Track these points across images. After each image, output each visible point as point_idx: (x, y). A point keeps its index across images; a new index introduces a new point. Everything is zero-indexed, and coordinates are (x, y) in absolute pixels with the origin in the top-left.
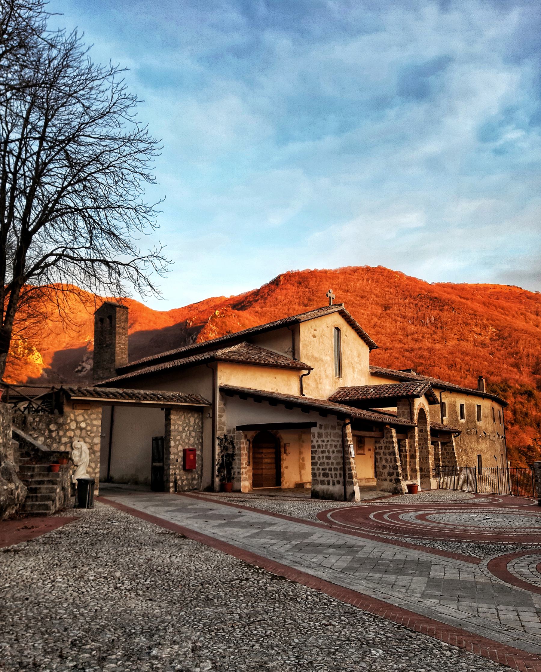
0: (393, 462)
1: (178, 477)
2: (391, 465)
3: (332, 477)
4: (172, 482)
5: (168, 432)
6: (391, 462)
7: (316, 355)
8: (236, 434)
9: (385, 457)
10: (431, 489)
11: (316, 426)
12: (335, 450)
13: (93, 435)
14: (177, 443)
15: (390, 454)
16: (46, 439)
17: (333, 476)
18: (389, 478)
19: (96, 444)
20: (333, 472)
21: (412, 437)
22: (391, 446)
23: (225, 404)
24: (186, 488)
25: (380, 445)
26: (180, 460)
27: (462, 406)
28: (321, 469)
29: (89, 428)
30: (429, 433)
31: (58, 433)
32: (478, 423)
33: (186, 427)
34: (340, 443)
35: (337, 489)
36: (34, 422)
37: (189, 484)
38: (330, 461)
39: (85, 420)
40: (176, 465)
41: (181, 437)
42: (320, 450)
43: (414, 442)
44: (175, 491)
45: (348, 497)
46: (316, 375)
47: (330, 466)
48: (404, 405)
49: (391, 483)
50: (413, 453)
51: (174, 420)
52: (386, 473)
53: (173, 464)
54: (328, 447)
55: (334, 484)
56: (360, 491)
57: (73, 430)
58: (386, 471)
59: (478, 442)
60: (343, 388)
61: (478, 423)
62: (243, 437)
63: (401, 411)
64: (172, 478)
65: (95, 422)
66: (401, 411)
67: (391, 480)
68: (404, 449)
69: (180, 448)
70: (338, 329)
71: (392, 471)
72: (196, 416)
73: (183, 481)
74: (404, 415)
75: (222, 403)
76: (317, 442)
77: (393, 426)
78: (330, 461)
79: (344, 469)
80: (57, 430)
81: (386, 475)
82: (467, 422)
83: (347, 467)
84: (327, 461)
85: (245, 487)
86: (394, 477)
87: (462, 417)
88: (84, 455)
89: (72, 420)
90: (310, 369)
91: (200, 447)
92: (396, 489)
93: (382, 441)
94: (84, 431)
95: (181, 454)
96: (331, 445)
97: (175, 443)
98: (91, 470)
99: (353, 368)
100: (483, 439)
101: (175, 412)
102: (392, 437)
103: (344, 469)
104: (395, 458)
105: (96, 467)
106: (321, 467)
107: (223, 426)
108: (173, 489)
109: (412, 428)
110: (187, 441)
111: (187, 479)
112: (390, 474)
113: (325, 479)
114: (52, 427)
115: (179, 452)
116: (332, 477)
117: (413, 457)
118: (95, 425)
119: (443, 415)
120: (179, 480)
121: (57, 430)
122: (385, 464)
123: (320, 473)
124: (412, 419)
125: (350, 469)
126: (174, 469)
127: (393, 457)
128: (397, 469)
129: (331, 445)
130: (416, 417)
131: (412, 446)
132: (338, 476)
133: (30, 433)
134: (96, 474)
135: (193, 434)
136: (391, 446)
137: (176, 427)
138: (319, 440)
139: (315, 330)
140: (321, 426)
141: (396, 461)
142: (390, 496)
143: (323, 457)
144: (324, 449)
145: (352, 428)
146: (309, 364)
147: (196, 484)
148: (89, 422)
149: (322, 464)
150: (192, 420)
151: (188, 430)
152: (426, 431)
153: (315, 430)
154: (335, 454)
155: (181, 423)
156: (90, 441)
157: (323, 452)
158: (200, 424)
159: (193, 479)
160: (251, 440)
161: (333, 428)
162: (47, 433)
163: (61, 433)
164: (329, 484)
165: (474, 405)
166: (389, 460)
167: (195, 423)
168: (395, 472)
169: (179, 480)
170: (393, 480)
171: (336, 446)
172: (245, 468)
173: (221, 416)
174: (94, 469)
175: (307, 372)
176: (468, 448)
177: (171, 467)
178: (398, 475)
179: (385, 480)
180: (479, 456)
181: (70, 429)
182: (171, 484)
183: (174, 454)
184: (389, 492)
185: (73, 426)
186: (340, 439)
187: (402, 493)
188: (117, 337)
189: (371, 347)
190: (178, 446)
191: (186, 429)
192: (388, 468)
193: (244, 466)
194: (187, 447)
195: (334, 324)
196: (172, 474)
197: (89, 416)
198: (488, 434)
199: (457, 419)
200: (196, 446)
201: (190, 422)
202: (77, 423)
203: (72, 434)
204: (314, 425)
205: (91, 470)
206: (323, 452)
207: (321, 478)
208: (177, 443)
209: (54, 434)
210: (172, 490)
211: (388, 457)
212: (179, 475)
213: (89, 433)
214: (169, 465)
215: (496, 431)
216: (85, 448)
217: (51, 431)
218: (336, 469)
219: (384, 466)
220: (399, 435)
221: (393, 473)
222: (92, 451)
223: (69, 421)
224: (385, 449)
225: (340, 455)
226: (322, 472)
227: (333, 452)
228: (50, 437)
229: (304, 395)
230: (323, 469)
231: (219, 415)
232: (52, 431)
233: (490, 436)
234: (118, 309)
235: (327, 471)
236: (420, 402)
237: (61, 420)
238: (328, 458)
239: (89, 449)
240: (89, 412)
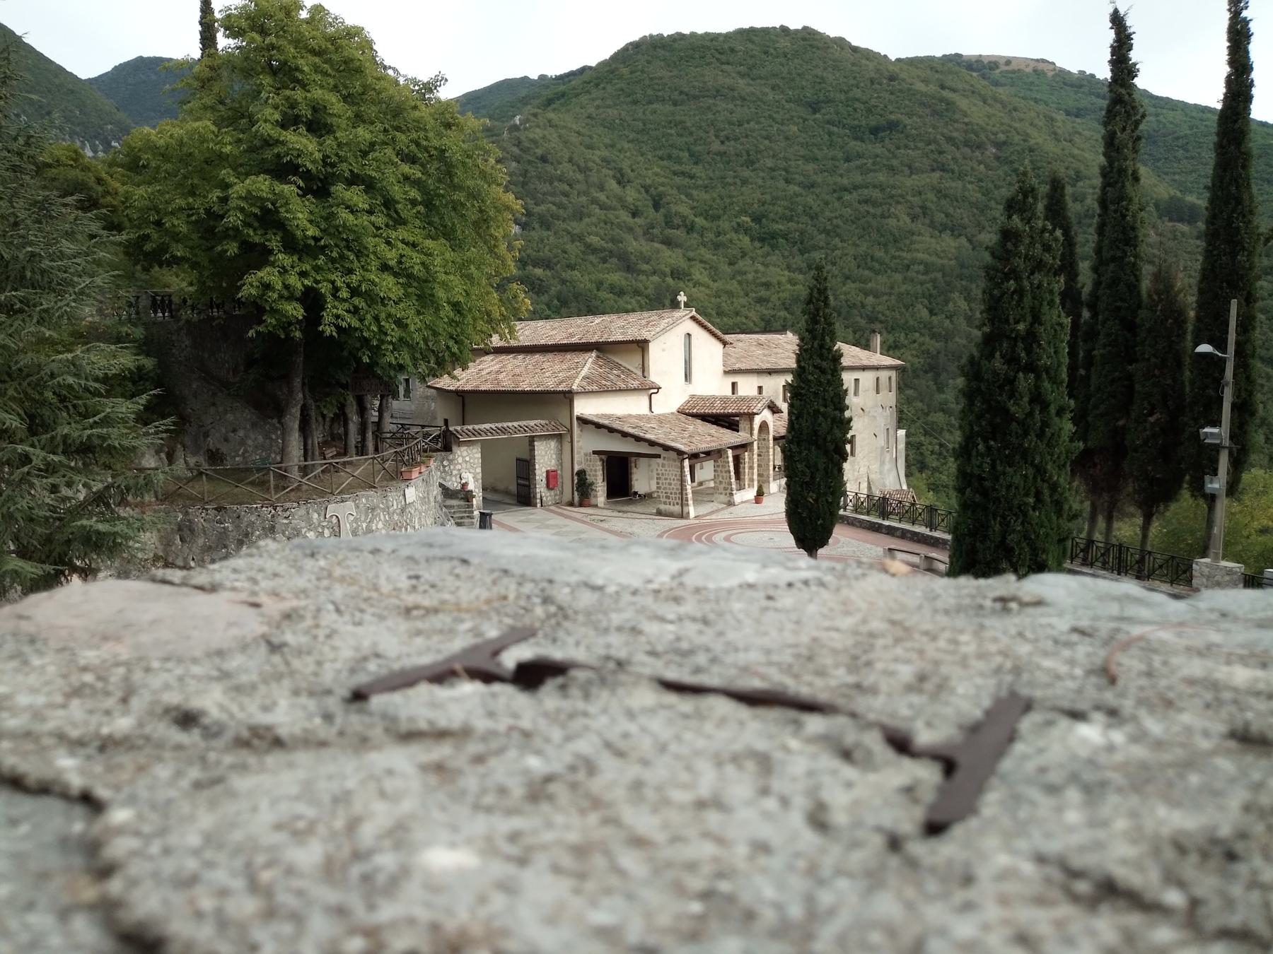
21: (752, 451)
35: (677, 509)
58: (722, 486)
60: (693, 396)
64: (538, 496)
86: (729, 491)
90: (659, 388)
114: (445, 463)
117: (751, 468)
124: (752, 434)
130: (756, 432)
131: (751, 459)
157: (666, 479)
161: (675, 461)
181: (458, 463)
185: (460, 460)
189: (725, 343)
198: (866, 410)
204: (658, 456)
206: (666, 479)
207: (664, 500)
209: (447, 469)
210: (539, 505)
217: (444, 466)
228: (444, 471)
237: (451, 457)
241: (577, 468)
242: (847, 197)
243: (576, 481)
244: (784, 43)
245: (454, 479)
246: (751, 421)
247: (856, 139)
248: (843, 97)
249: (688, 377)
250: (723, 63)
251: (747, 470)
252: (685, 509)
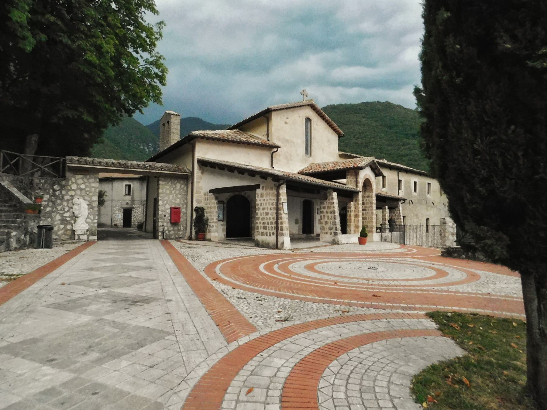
0: (333, 219)
1: (166, 228)
2: (332, 221)
3: (269, 230)
4: (160, 232)
5: (158, 194)
6: (331, 219)
7: (288, 138)
8: (209, 196)
9: (327, 215)
10: (373, 242)
11: (260, 188)
12: (272, 207)
13: (91, 194)
14: (165, 202)
15: (331, 213)
16: (51, 196)
17: (270, 228)
18: (329, 231)
19: (94, 202)
20: (270, 226)
21: (357, 201)
22: (332, 206)
23: (202, 173)
24: (173, 237)
25: (324, 205)
26: (167, 215)
27: (415, 183)
28: (262, 223)
29: (88, 189)
30: (374, 199)
31: (61, 192)
32: (428, 196)
33: (172, 191)
34: (275, 201)
35: (272, 239)
36: (40, 184)
37: (175, 234)
38: (268, 217)
39: (84, 183)
40: (164, 219)
41: (169, 198)
42: (261, 207)
43: (358, 204)
44: (163, 238)
45: (279, 246)
46: (287, 153)
47: (268, 221)
48: (351, 175)
49: (331, 236)
50: (357, 213)
51: (162, 185)
52: (328, 228)
53: (161, 218)
54: (268, 204)
55: (270, 235)
56: (291, 241)
57: (74, 190)
58: (327, 227)
59: (427, 209)
61: (428, 196)
62: (214, 198)
63: (349, 180)
65: (93, 185)
66: (349, 180)
67: (331, 234)
68: (349, 210)
69: (168, 206)
70: (308, 120)
71: (332, 226)
72: (182, 182)
73: (170, 231)
74: (351, 184)
75: (200, 172)
76: (260, 200)
77: (335, 190)
78: (268, 217)
79: (277, 223)
80: (61, 190)
81: (328, 229)
82: (419, 195)
83: (280, 221)
84: (266, 216)
85: (215, 237)
87: (415, 191)
88: (82, 209)
89: (73, 183)
90: (278, 147)
91: (185, 206)
92: (334, 240)
93: (325, 203)
94: (83, 191)
95: (169, 211)
96: (269, 203)
97: (163, 202)
98: (90, 221)
99: (323, 150)
100: (431, 207)
101: (163, 179)
102: (332, 199)
103: (277, 223)
104: (335, 216)
105: (94, 219)
107: (200, 190)
108: (162, 237)
109: (357, 193)
110: (174, 201)
111: (173, 230)
112: (330, 229)
113: (265, 231)
114: (56, 187)
115: (167, 209)
116: (269, 230)
117: (356, 216)
118: (93, 187)
119: (399, 188)
120: (166, 231)
121: (61, 190)
123: (261, 226)
124: (357, 186)
125: (282, 223)
126: (162, 222)
127: (333, 215)
128: (336, 225)
129: (269, 203)
130: (361, 185)
132: (273, 228)
133: (37, 191)
134: (94, 223)
135: (179, 196)
136: (332, 206)
137: (164, 190)
138: (262, 199)
139: (287, 118)
140: (263, 187)
141: (335, 218)
142: (330, 245)
143: (263, 213)
144: (264, 207)
145: (287, 188)
146: (277, 143)
147: (181, 234)
148: (88, 185)
149: (263, 219)
150: (178, 185)
151: (175, 193)
152: (372, 197)
153: (259, 191)
154: (272, 211)
155: (168, 187)
156: (89, 199)
158: (185, 188)
159: (179, 230)
160: (226, 201)
161: (271, 189)
162: (51, 191)
163: (64, 192)
164: (267, 235)
165: (425, 183)
166: (330, 217)
167: (181, 187)
168: (334, 227)
169: (166, 231)
170: (333, 233)
171: (272, 204)
172: (215, 223)
173: (198, 182)
174: (92, 220)
175: (276, 149)
176: (419, 214)
177: (160, 220)
178: (336, 229)
179: (327, 233)
180: (427, 219)
181: (71, 189)
182: (160, 234)
183: (162, 211)
184: (329, 243)
185: (74, 187)
186: (276, 198)
187: (338, 244)
188: (172, 135)
190: (166, 204)
191: (173, 192)
192: (329, 224)
193: (215, 220)
194: (173, 206)
195: (306, 115)
196: (161, 226)
197: (88, 180)
198: (435, 204)
199: (411, 192)
200: (181, 205)
201: (176, 187)
202: (78, 184)
203: (72, 193)
204: (258, 186)
205: (90, 221)
206: (264, 209)
208: (165, 202)
209: (57, 193)
210: (160, 238)
211: (330, 215)
212: (167, 227)
213: (88, 193)
214: (158, 219)
215: (442, 202)
216: (84, 205)
217: (54, 191)
218: (272, 223)
219: (326, 222)
220: (341, 198)
221: (333, 228)
222: (90, 206)
223: (70, 183)
224: (328, 209)
225: (275, 211)
226: (262, 225)
227: (271, 209)
228: (54, 195)
229: (273, 168)
230: (263, 223)
231: (196, 181)
232: (56, 191)
233: (437, 206)
234: (172, 116)
235: (266, 225)
236: (366, 173)
237: (64, 183)
238: (267, 214)
239: (88, 205)
240: (88, 177)
241: (195, 205)
242: (404, 158)
243: (194, 217)
244: (379, 106)
245: (65, 203)
246: (356, 175)
247: (407, 138)
248: (401, 124)
249: (308, 150)
250: (356, 113)
251: (353, 218)
252: (280, 239)
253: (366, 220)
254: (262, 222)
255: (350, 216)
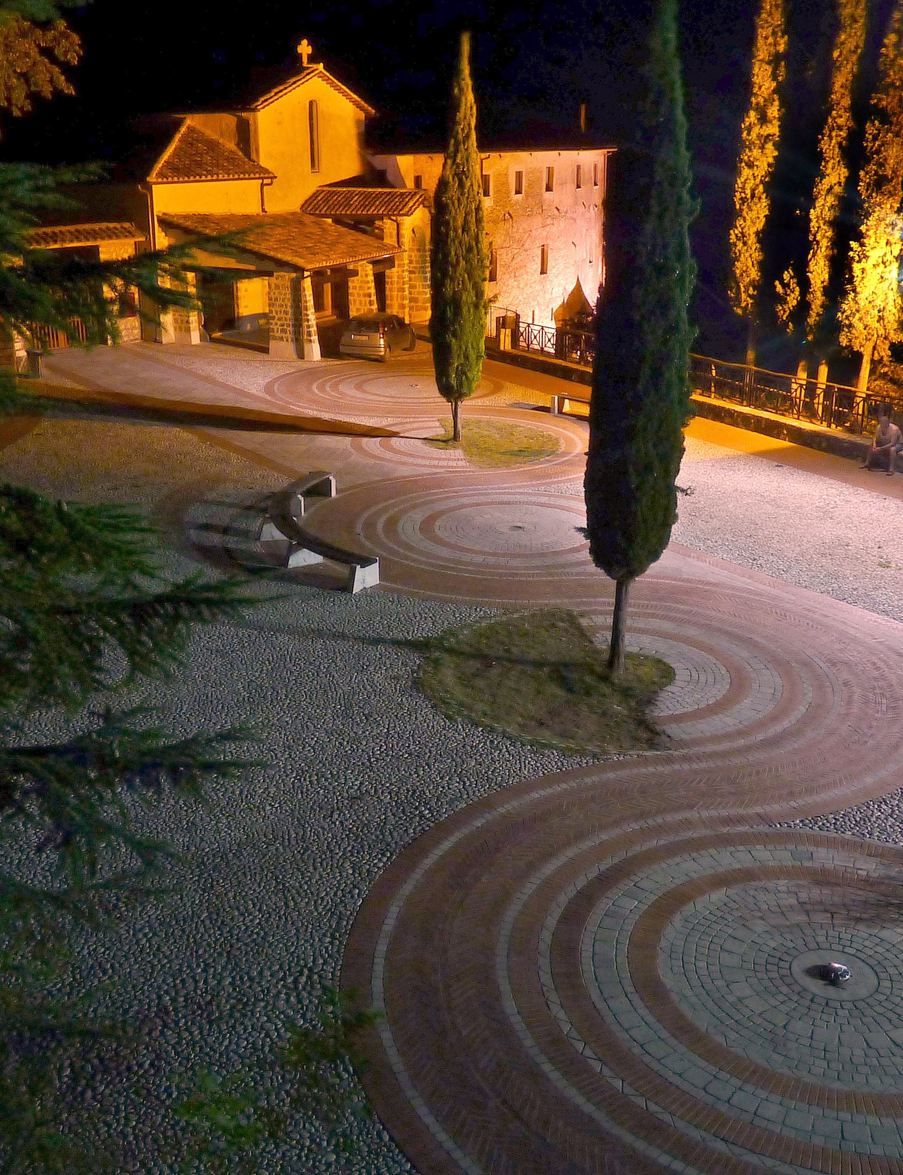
15: (365, 295)
27: (519, 175)
82: (527, 196)
106: (279, 323)
122: (359, 307)
123: (278, 329)
127: (368, 299)
149: (279, 319)
166: (363, 302)
211: (363, 299)
229: (266, 212)
235: (285, 327)
253: (416, 288)
254: (279, 323)
255: (391, 290)
